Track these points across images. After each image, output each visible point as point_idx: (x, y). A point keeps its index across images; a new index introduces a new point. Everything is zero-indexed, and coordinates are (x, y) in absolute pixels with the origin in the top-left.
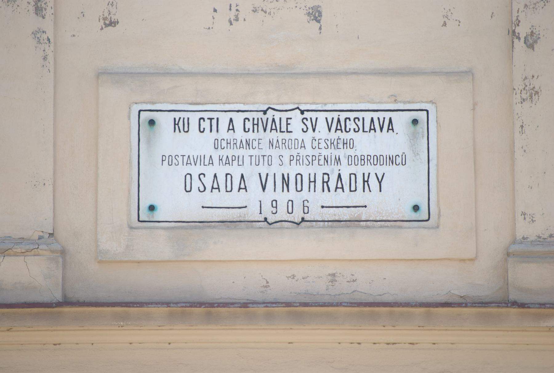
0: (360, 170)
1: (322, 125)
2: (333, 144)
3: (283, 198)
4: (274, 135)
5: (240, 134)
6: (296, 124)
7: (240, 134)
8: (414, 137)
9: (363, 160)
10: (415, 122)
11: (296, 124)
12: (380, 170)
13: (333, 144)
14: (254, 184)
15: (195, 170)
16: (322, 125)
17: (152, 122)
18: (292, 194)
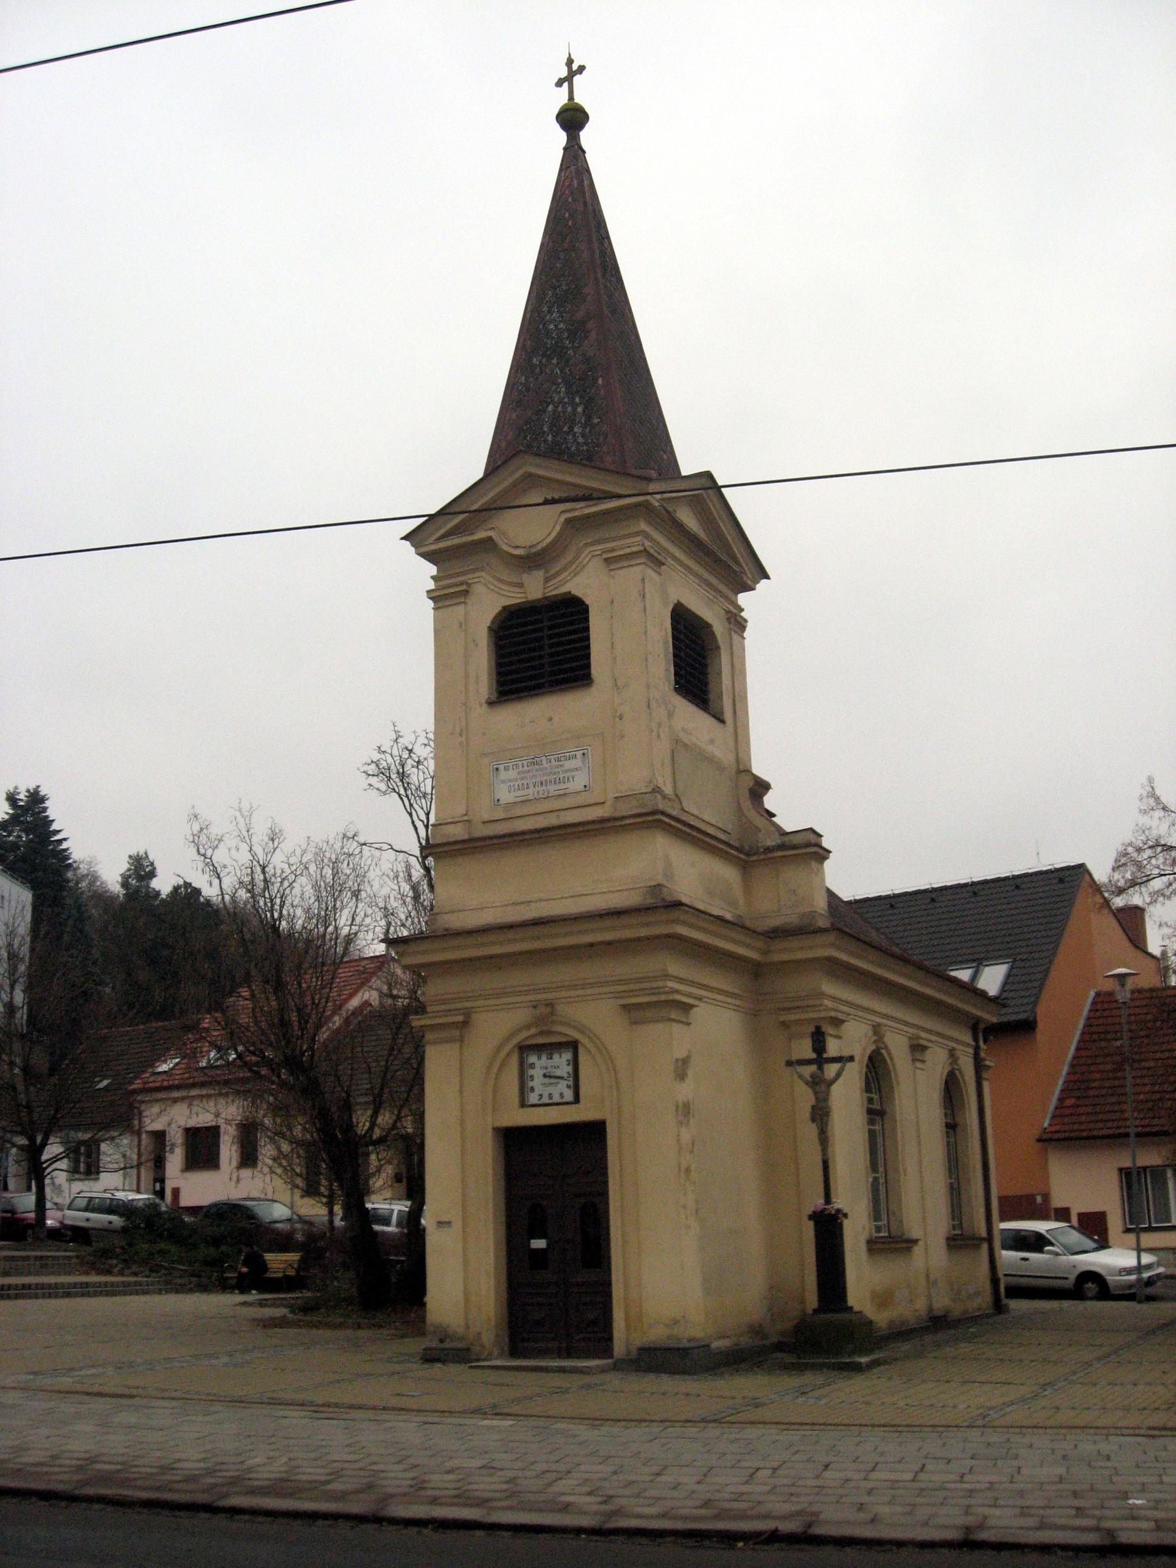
0: (566, 775)
1: (553, 761)
2: (557, 767)
3: (541, 789)
4: (537, 767)
5: (526, 768)
6: (544, 762)
7: (526, 768)
8: (583, 762)
9: (567, 771)
10: (584, 754)
11: (544, 762)
12: (573, 773)
13: (557, 767)
14: (531, 786)
15: (511, 784)
16: (553, 761)
17: (497, 769)
18: (544, 788)
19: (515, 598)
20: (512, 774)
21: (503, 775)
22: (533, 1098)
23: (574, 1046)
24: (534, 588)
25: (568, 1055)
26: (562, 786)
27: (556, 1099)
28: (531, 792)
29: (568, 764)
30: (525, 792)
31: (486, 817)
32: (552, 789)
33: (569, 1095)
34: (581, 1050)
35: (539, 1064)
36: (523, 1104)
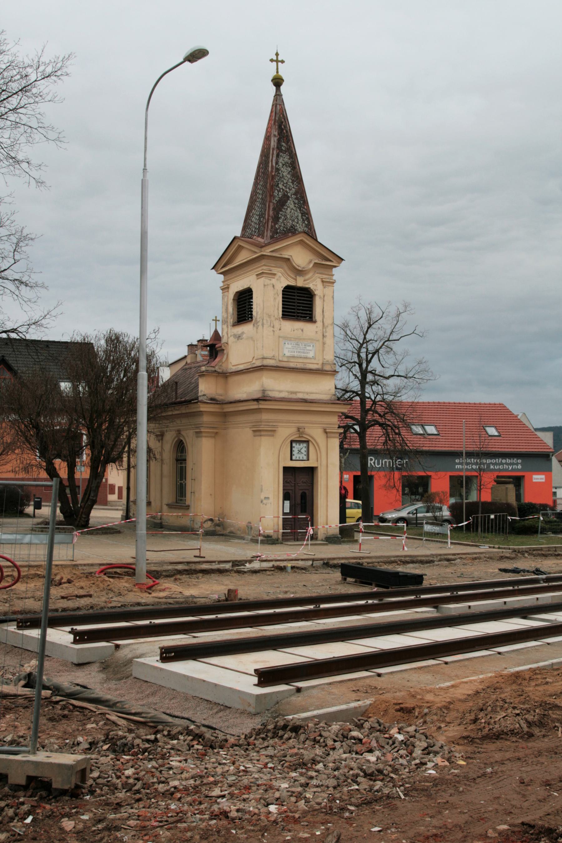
19: (292, 283)
20: (290, 346)
21: (287, 346)
22: (294, 458)
23: (307, 442)
24: (300, 282)
25: (305, 445)
26: (305, 355)
27: (301, 459)
28: (296, 354)
29: (308, 348)
30: (294, 354)
31: (281, 359)
32: (302, 355)
33: (305, 458)
34: (310, 444)
35: (296, 447)
36: (291, 459)
